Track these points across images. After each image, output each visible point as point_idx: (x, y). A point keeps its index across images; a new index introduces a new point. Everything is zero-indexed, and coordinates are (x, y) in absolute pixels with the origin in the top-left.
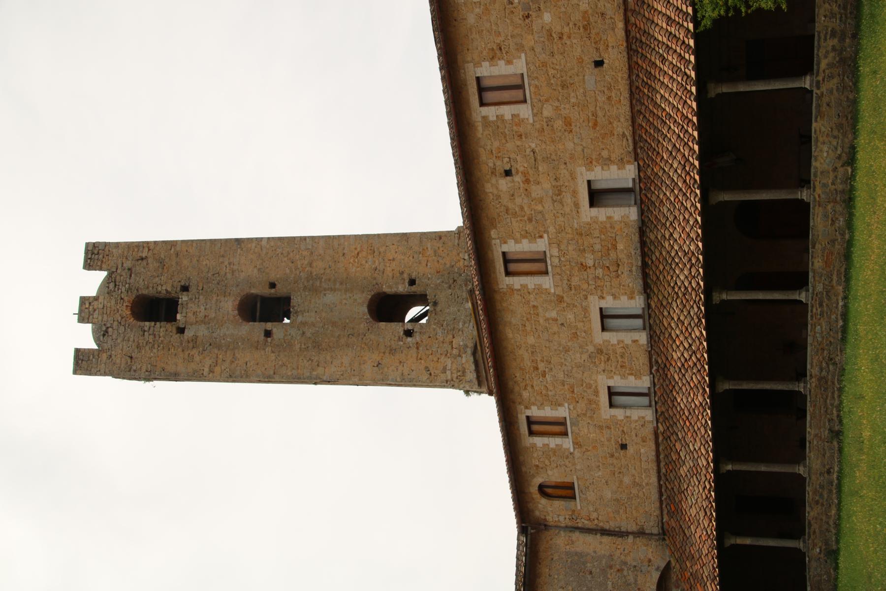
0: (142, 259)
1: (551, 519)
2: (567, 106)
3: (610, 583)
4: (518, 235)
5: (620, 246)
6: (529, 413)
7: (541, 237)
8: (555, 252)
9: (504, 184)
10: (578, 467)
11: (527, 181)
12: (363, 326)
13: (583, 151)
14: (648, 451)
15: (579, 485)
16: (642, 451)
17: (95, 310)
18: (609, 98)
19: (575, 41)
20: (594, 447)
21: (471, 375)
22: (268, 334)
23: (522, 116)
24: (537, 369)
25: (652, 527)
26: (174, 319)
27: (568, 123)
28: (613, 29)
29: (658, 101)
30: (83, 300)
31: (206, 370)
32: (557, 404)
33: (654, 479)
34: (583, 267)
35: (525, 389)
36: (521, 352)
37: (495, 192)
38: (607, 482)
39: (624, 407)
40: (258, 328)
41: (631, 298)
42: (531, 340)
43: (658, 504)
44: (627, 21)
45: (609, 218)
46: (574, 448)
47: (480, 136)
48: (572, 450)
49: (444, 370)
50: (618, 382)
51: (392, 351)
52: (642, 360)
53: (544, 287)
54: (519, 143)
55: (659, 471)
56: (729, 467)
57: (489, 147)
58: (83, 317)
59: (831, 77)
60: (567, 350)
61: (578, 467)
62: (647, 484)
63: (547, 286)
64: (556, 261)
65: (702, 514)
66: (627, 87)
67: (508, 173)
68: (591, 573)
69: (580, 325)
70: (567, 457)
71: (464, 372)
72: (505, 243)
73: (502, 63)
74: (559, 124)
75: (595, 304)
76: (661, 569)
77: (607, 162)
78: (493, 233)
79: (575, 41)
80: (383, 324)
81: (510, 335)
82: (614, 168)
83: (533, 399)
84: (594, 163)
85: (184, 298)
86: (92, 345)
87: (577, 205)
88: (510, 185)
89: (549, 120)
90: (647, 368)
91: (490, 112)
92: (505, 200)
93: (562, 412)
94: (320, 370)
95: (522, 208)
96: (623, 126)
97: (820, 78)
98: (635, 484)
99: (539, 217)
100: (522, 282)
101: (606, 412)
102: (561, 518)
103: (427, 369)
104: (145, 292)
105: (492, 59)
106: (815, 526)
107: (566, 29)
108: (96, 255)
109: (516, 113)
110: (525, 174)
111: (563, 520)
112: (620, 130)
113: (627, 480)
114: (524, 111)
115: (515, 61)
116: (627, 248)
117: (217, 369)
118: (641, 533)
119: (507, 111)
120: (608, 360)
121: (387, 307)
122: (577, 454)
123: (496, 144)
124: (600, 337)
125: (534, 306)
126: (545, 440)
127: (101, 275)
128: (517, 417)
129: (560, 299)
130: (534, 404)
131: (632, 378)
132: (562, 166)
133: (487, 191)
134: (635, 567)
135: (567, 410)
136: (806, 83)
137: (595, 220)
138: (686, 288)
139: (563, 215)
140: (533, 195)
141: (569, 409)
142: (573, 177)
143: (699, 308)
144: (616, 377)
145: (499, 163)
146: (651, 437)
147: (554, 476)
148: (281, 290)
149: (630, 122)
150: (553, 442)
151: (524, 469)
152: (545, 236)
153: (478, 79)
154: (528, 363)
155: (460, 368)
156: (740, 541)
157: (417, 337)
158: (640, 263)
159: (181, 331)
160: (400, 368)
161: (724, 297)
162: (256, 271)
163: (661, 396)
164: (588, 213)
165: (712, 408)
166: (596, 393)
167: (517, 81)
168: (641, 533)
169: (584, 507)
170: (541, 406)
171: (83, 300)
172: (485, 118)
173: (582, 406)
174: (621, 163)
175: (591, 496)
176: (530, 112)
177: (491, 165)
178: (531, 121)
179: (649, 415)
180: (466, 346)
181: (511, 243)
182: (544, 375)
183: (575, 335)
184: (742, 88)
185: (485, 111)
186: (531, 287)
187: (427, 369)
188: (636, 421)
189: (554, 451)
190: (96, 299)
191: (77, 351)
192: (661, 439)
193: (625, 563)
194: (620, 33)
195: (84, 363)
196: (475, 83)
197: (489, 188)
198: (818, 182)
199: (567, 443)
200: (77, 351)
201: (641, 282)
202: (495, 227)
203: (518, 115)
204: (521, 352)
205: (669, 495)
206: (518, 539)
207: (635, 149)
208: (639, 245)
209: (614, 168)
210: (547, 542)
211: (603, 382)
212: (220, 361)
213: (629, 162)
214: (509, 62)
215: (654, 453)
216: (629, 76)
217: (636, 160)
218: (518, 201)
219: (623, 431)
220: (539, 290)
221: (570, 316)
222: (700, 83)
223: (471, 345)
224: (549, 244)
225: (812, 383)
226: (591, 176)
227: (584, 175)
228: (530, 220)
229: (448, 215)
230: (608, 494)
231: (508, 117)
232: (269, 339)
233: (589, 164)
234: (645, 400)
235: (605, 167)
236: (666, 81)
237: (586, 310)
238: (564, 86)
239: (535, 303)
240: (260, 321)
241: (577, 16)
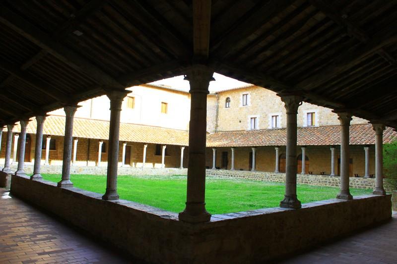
1: (220, 100)
6: (249, 94)
24: (261, 97)
33: (231, 130)
39: (251, 122)
42: (270, 95)
44: (360, 125)
50: (257, 120)
52: (264, 127)
55: (233, 131)
56: (232, 151)
59: (333, 180)
60: (267, 106)
69: (273, 110)
87: (308, 109)
97: (333, 177)
106: (218, 171)
111: (220, 105)
112: (329, 122)
113: (231, 122)
122: (238, 109)
124: (270, 115)
126: (242, 99)
136: (332, 174)
137: (303, 114)
146: (244, 129)
150: (241, 102)
154: (263, 95)
161: (277, 151)
163: (254, 133)
166: (255, 114)
168: (217, 126)
169: (223, 111)
170: (251, 98)
173: (251, 110)
175: (227, 112)
179: (249, 129)
182: (260, 99)
183: (271, 108)
184: (332, 157)
198: (306, 176)
199: (241, 106)
205: (227, 134)
207: (323, 126)
211: (258, 116)
221: (276, 107)
225: (254, 173)
230: (227, 117)
237: (278, 111)
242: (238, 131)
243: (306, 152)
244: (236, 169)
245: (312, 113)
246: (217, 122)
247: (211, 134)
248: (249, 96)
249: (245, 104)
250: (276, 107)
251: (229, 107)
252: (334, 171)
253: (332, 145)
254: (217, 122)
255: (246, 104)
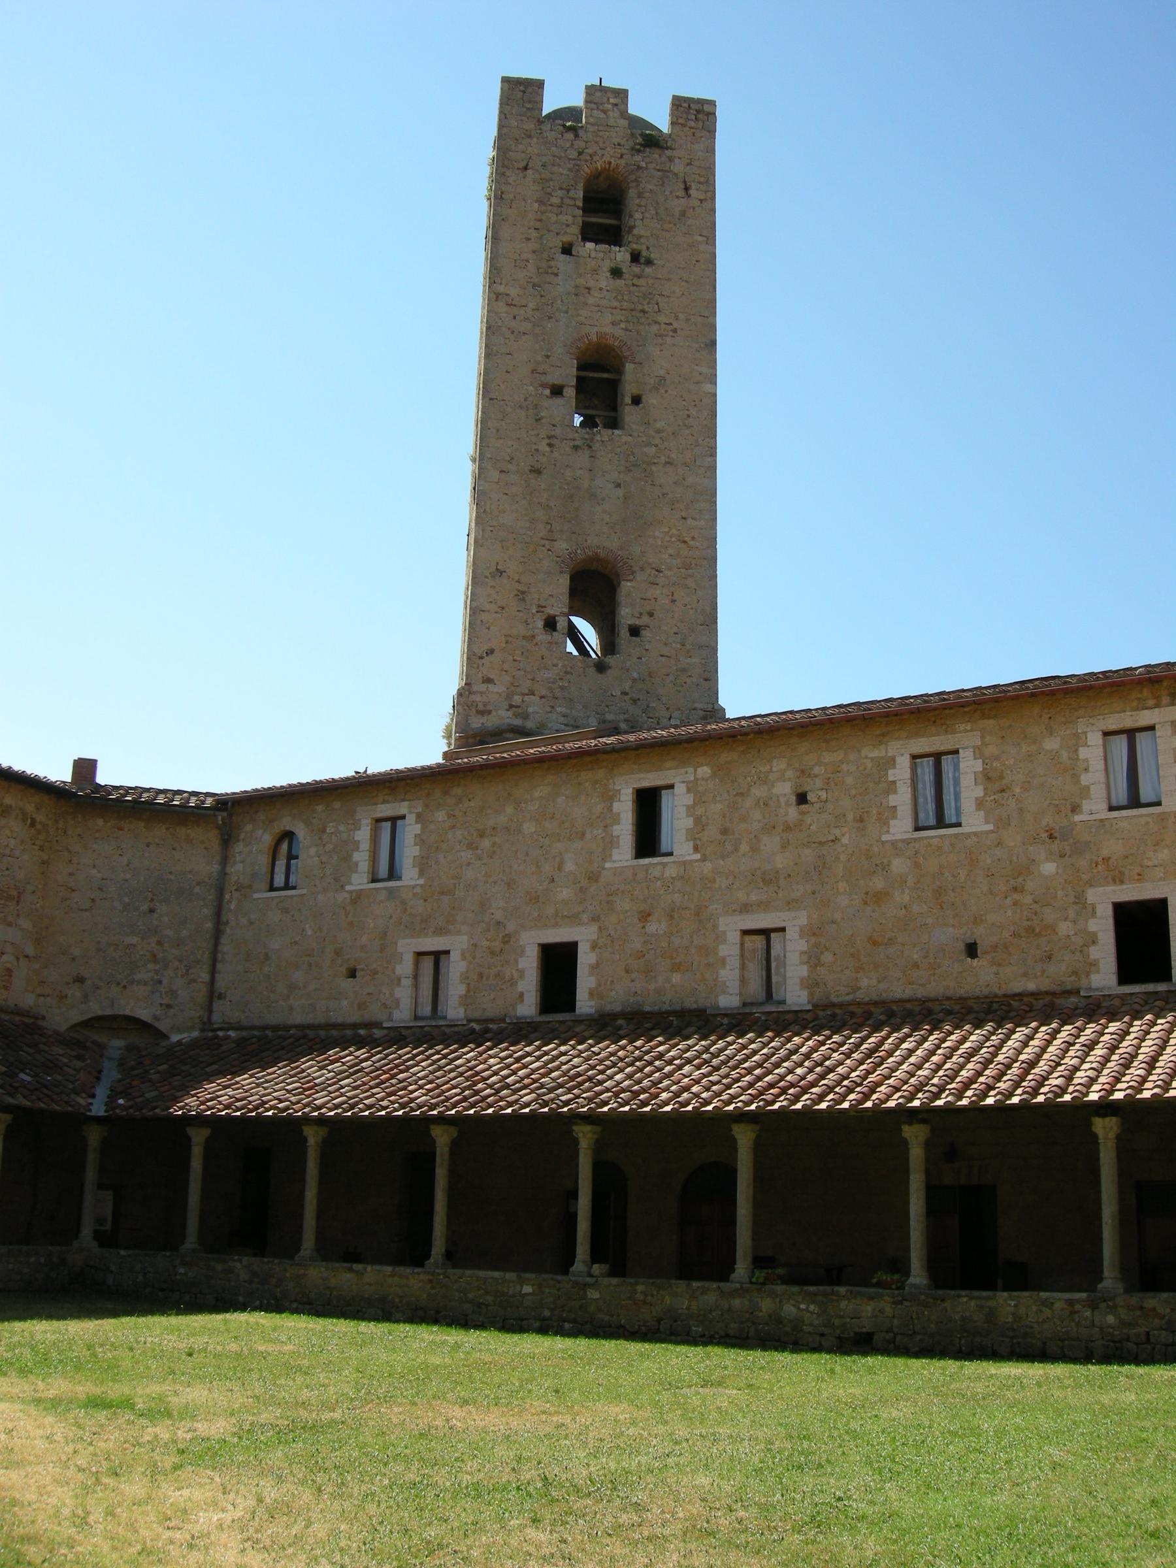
0: (687, 189)
1: (239, 848)
2: (906, 898)
3: (134, 940)
4: (699, 811)
5: (676, 978)
6: (411, 819)
7: (696, 849)
8: (670, 872)
9: (785, 789)
10: (320, 897)
11: (787, 828)
12: (562, 546)
13: (833, 922)
14: (345, 1011)
15: (292, 897)
16: (345, 1003)
17: (605, 112)
18: (916, 966)
19: (1009, 913)
20: (351, 924)
21: (477, 723)
22: (557, 391)
23: (892, 822)
24: (482, 835)
25: (223, 1012)
26: (586, 238)
27: (879, 897)
28: (1025, 975)
29: (905, 1046)
30: (622, 94)
31: (501, 289)
32: (423, 865)
33: (298, 1018)
34: (645, 916)
35: (450, 816)
36: (509, 810)
37: (772, 777)
38: (296, 943)
39: (416, 977)
40: (567, 374)
41: (591, 994)
42: (529, 827)
43: (257, 1023)
44: (1035, 995)
45: (723, 962)
46: (351, 892)
47: (864, 752)
48: (348, 888)
49: (488, 681)
50: (456, 967)
51: (521, 596)
52: (490, 1005)
53: (615, 851)
54: (850, 817)
55: (310, 1027)
56: (311, 1141)
57: (844, 767)
58: (595, 93)
61: (320, 897)
62: (291, 1008)
63: (615, 857)
64: (656, 872)
65: (239, 1093)
66: (933, 994)
67: (802, 799)
68: (152, 911)
69: (550, 911)
70: (336, 880)
71: (482, 713)
72: (689, 790)
73: (979, 792)
74: (878, 883)
75: (582, 935)
76: (157, 1024)
77: (813, 959)
78: (705, 771)
79: (1009, 913)
80: (564, 581)
81: (537, 794)
82: (804, 971)
83: (432, 827)
84: (813, 940)
85: (621, 255)
86: (550, 105)
87: (745, 908)
88: (782, 800)
89: (885, 867)
90: (478, 1014)
91: (901, 772)
92: (758, 792)
93: (410, 875)
94: (495, 475)
95: (744, 819)
96: (870, 986)
98: (293, 987)
99: (729, 847)
100: (623, 816)
101: (407, 946)
102: (239, 867)
103: (490, 652)
104: (632, 193)
105: (986, 778)
107: (1028, 899)
108: (695, 115)
109: (899, 813)
110: (799, 825)
111: (237, 870)
112: (865, 982)
113: (298, 976)
114: (901, 827)
115: (982, 813)
116: (673, 987)
117: (501, 307)
118: (213, 995)
119: (902, 798)
120: (493, 953)
121: (594, 587)
122: (341, 897)
123: (849, 780)
125: (583, 834)
126: (365, 845)
127: (661, 120)
128: (403, 800)
129: (593, 877)
130: (423, 828)
131: (461, 989)
132: (809, 888)
133: (775, 762)
134: (160, 982)
135: (412, 883)
137: (720, 938)
138: (600, 1083)
139: (729, 887)
140: (765, 839)
141: (414, 887)
142: (791, 904)
143: (567, 1103)
144: (463, 964)
145: (819, 783)
146: (368, 1017)
147: (309, 854)
148: (630, 415)
149: (875, 998)
150: (361, 858)
151: (320, 808)
152: (698, 856)
153: (956, 752)
155: (489, 708)
156: (197, 1151)
157: (543, 637)
158: (647, 1008)
159: (567, 250)
160: (494, 607)
162: (662, 373)
164: (731, 926)
165: (406, 1119)
166: (440, 931)
167: (950, 816)
170: (420, 840)
171: (622, 94)
172: (891, 762)
174: (810, 984)
176: (899, 837)
177: (816, 770)
178: (885, 838)
180: (526, 716)
181: (689, 800)
182: (471, 846)
185: (904, 762)
186: (616, 830)
187: (490, 652)
188: (392, 994)
189: (347, 858)
190: (624, 113)
191: (540, 84)
192: (362, 1032)
193: (166, 967)
194: (1017, 986)
195: (520, 94)
196: (949, 747)
197: (779, 765)
199: (359, 881)
200: (540, 84)
201: (618, 1008)
202: (714, 775)
203: (895, 817)
204: (509, 810)
206: (208, 794)
207: (834, 1005)
208: (678, 1008)
209: (804, 971)
210: (202, 842)
211: (457, 944)
212: (515, 311)
213: (811, 995)
214: (980, 804)
215: (340, 1020)
216: (949, 999)
217: (815, 1006)
218: (756, 815)
219: (376, 973)
220: (611, 842)
222: (925, 1115)
223: (530, 725)
224: (684, 863)
226: (792, 933)
227: (795, 921)
228: (724, 831)
229: (743, 693)
231: (893, 800)
232: (547, 392)
233: (811, 932)
234: (427, 1010)
235: (805, 958)
236: (935, 1059)
237: (575, 920)
238: (939, 892)
239: (588, 836)
240: (580, 379)
241: (1049, 916)
242: (335, 1026)
243: (758, 1147)
244: (328, 1251)
245: (766, 933)
246: (213, 972)
247: (175, 1038)
248: (410, 830)
249: (383, 870)
250: (565, 893)
251: (287, 886)
252: (934, 1265)
253: (914, 1110)
254: (213, 972)
255: (393, 874)
